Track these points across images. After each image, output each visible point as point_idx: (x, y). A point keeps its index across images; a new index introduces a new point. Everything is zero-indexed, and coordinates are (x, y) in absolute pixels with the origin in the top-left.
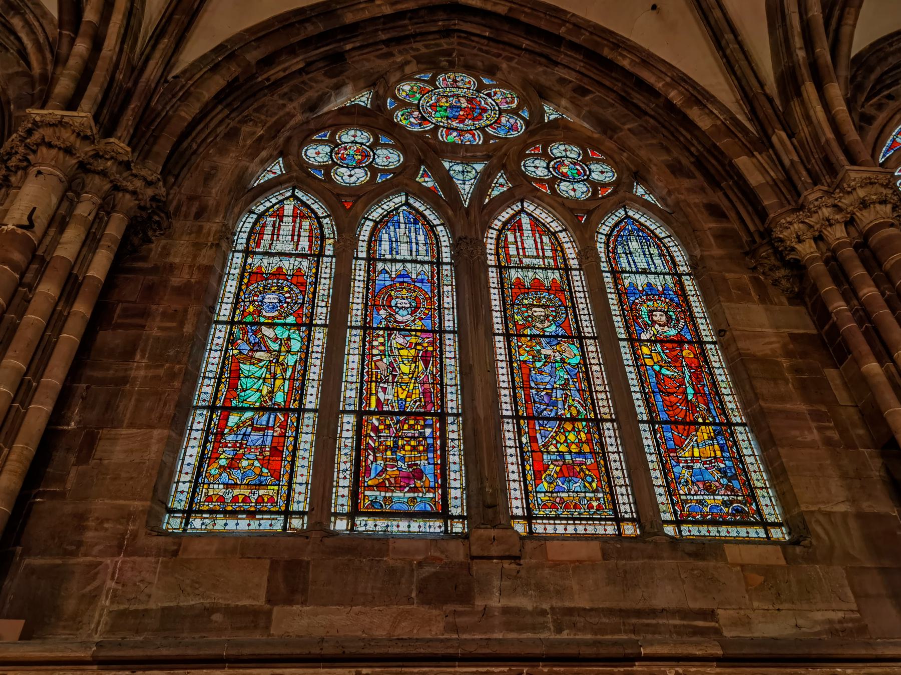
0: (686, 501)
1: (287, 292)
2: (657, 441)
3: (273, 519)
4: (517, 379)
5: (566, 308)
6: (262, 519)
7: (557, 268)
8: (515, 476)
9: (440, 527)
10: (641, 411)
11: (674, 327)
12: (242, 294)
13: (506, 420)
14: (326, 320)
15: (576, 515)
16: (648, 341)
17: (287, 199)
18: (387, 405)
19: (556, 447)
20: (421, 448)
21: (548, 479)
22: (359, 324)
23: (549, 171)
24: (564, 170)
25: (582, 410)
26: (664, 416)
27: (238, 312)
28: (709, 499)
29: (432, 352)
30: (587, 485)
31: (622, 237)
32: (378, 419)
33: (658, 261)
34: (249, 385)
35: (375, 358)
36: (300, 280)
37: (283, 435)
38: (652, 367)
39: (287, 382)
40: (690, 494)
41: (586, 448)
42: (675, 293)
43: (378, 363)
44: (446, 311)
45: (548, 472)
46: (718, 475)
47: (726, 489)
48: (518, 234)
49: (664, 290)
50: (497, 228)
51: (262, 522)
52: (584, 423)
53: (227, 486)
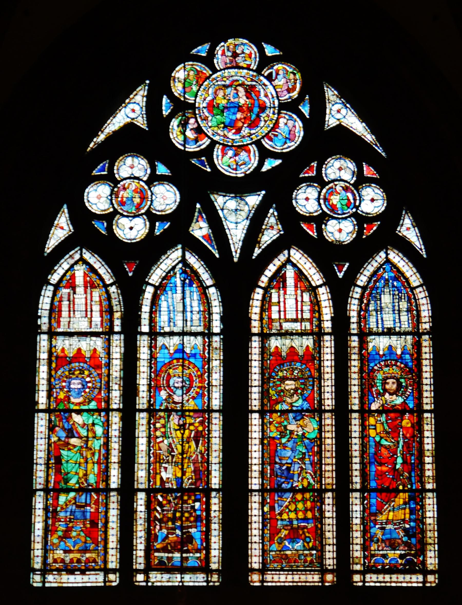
0: (373, 556)
1: (88, 376)
2: (364, 507)
3: (98, 574)
4: (266, 455)
5: (314, 378)
6: (90, 574)
7: (311, 333)
8: (256, 539)
9: (204, 578)
10: (357, 479)
11: (401, 396)
12: (52, 380)
13: (254, 493)
14: (119, 404)
15: (294, 568)
16: (377, 411)
17: (76, 263)
18: (168, 483)
19: (288, 515)
20: (192, 519)
21: (279, 541)
22: (145, 406)
23: (320, 204)
24: (335, 200)
25: (312, 481)
26: (373, 484)
27: (52, 399)
28: (392, 554)
29: (202, 431)
30: (306, 544)
31: (377, 288)
32: (162, 496)
33: (404, 318)
34: (69, 469)
35: (158, 440)
36: (97, 363)
37: (97, 509)
38: (374, 438)
39: (96, 465)
40: (378, 550)
41: (309, 515)
42: (411, 355)
43: (161, 445)
44: (214, 389)
45: (279, 535)
46: (402, 534)
47: (405, 546)
48: (282, 292)
49: (402, 353)
50: (263, 285)
51: (90, 576)
52: (311, 494)
53: (65, 552)
